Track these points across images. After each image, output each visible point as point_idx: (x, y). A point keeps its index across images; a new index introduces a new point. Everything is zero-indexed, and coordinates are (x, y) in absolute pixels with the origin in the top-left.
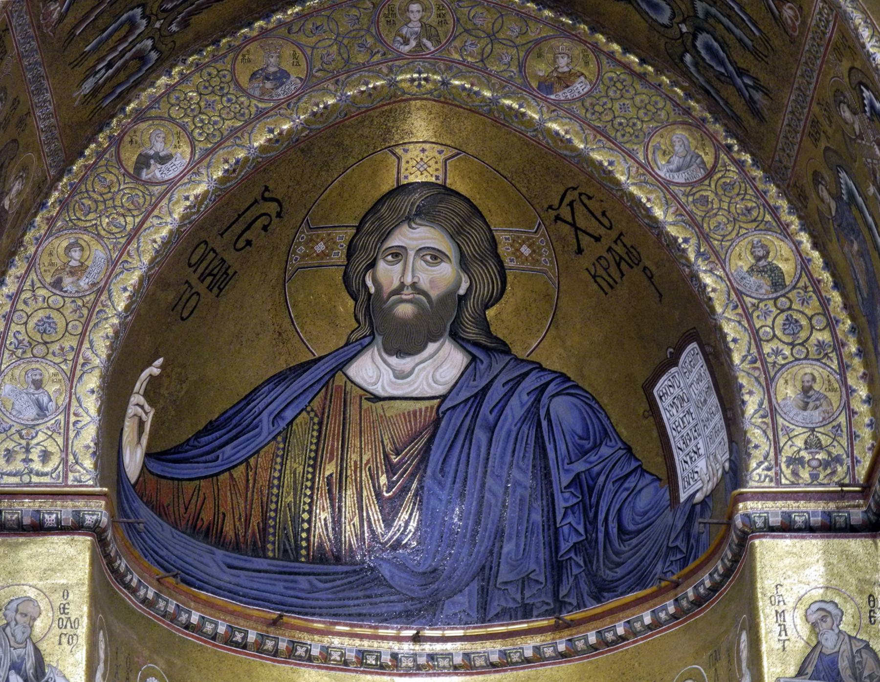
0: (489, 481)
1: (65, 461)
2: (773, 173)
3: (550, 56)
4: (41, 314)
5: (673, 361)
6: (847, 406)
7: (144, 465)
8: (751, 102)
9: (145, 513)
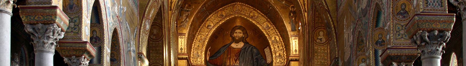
0: (247, 58)
1: (201, 62)
2: (277, 28)
3: (253, 13)
4: (198, 45)
5: (266, 48)
6: (284, 56)
7: (209, 59)
8: (274, 22)
9: (209, 64)
